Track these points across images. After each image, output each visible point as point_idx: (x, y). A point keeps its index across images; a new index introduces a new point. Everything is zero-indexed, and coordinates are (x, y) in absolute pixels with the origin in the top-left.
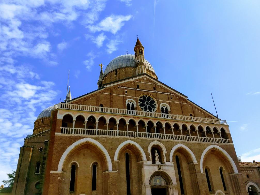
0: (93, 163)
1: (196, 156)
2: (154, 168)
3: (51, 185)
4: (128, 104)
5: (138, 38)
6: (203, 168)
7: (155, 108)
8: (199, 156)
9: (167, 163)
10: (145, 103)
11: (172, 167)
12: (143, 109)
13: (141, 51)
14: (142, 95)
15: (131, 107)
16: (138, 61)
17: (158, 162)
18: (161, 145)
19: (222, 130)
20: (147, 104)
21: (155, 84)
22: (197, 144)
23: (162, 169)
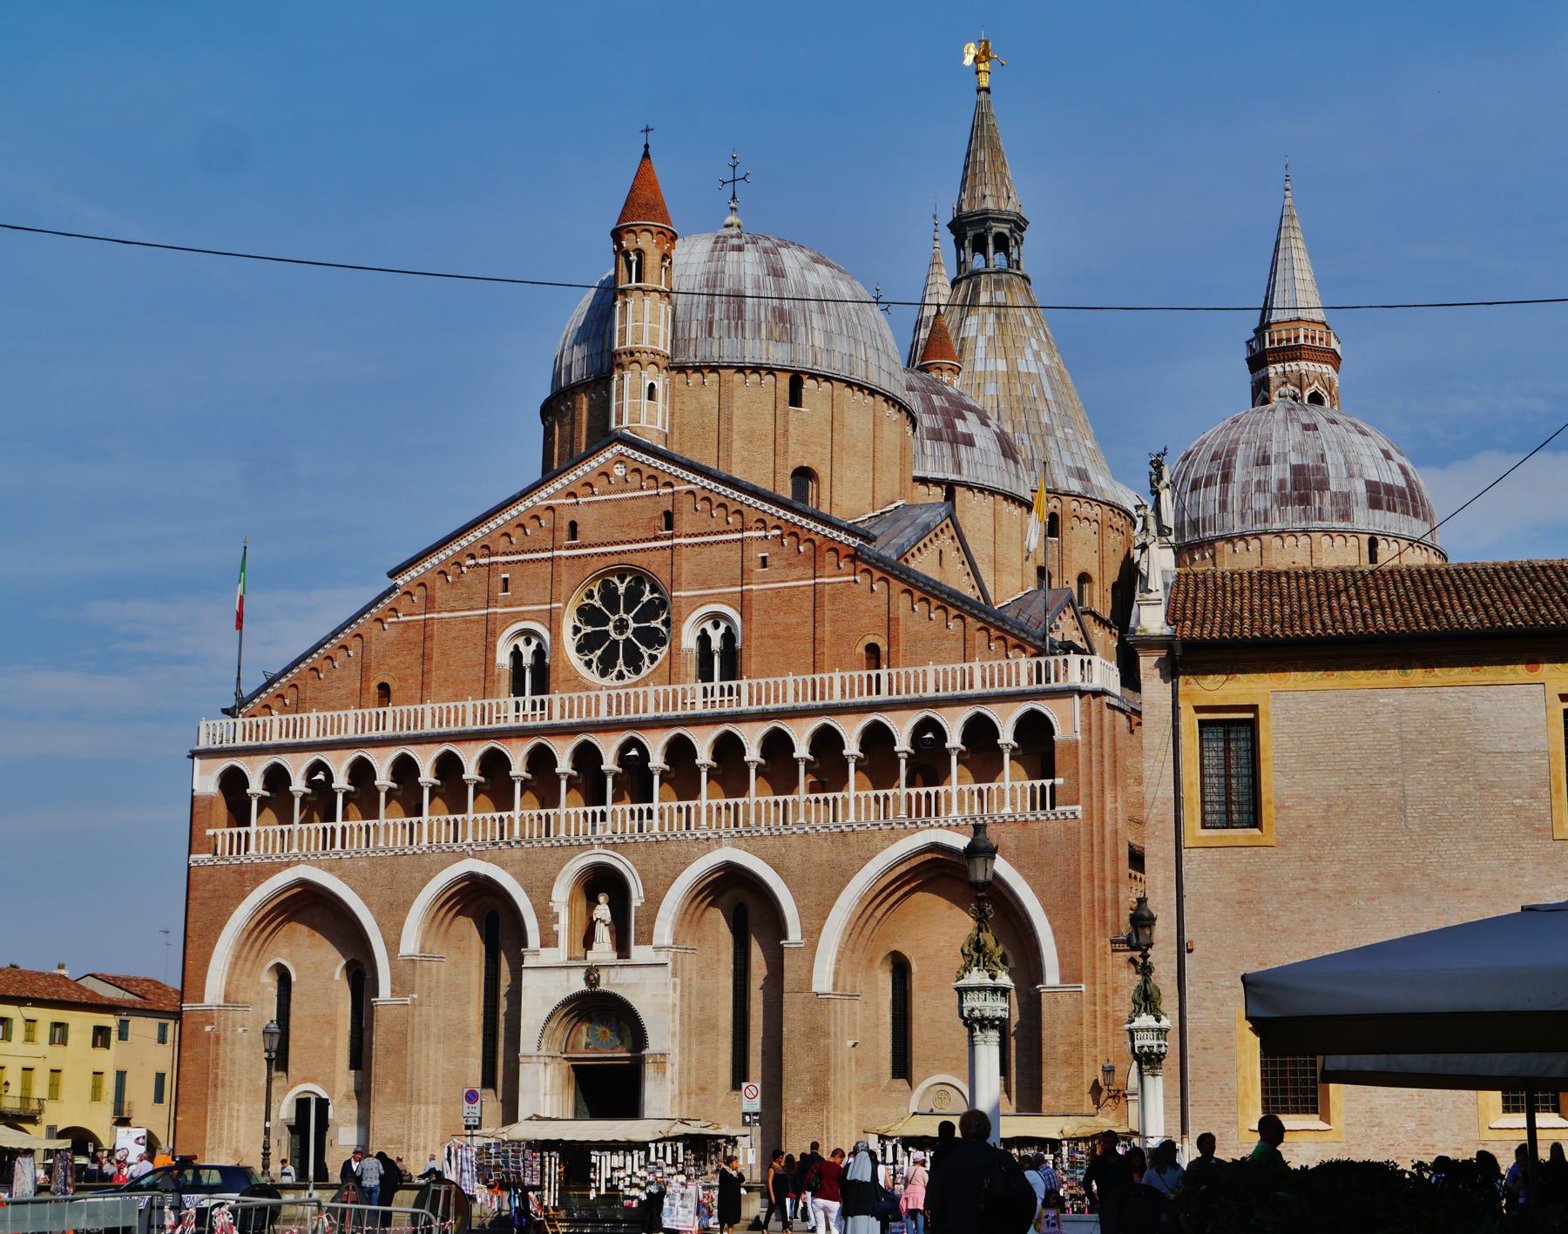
1: (801, 904)
2: (568, 979)
5: (647, 146)
10: (611, 624)
11: (659, 968)
12: (594, 665)
13: (633, 257)
15: (532, 668)
18: (622, 864)
20: (621, 626)
21: (672, 486)
22: (826, 839)
23: (603, 981)
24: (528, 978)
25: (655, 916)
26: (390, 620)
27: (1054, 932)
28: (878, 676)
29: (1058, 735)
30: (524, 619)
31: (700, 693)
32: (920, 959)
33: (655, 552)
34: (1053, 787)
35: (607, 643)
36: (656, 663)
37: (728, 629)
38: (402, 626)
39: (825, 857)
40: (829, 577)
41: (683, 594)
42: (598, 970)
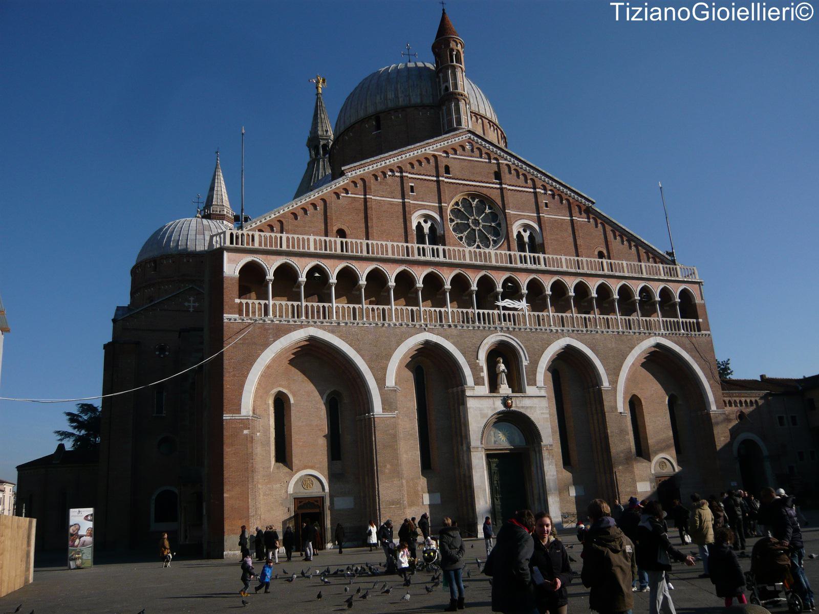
0: (328, 392)
3: (228, 450)
5: (443, 10)
6: (624, 398)
8: (614, 369)
11: (542, 399)
12: (464, 240)
13: (455, 53)
14: (458, 198)
16: (447, 88)
18: (514, 341)
19: (685, 294)
20: (476, 223)
23: (514, 405)
24: (471, 404)
25: (536, 371)
26: (342, 194)
27: (710, 387)
30: (425, 209)
32: (645, 398)
33: (492, 189)
34: (698, 323)
35: (469, 230)
38: (351, 199)
39: (613, 346)
40: (578, 218)
41: (512, 212)
42: (511, 399)
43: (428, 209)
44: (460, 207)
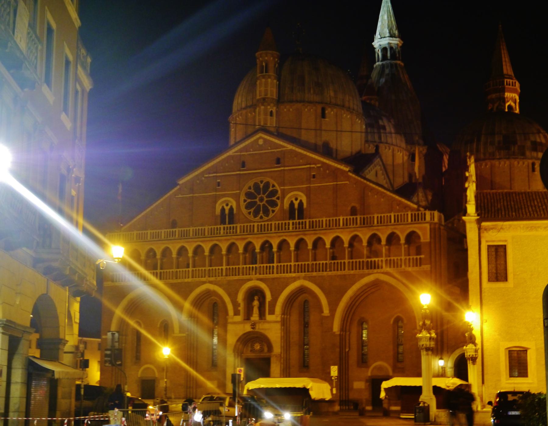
4: (223, 210)
7: (277, 205)
9: (269, 317)
10: (258, 198)
12: (252, 214)
14: (251, 183)
17: (255, 317)
18: (263, 286)
20: (261, 200)
23: (257, 327)
24: (230, 327)
26: (177, 196)
28: (356, 218)
29: (422, 240)
31: (291, 224)
34: (420, 258)
36: (275, 213)
37: (301, 201)
43: (228, 197)
44: (252, 191)
